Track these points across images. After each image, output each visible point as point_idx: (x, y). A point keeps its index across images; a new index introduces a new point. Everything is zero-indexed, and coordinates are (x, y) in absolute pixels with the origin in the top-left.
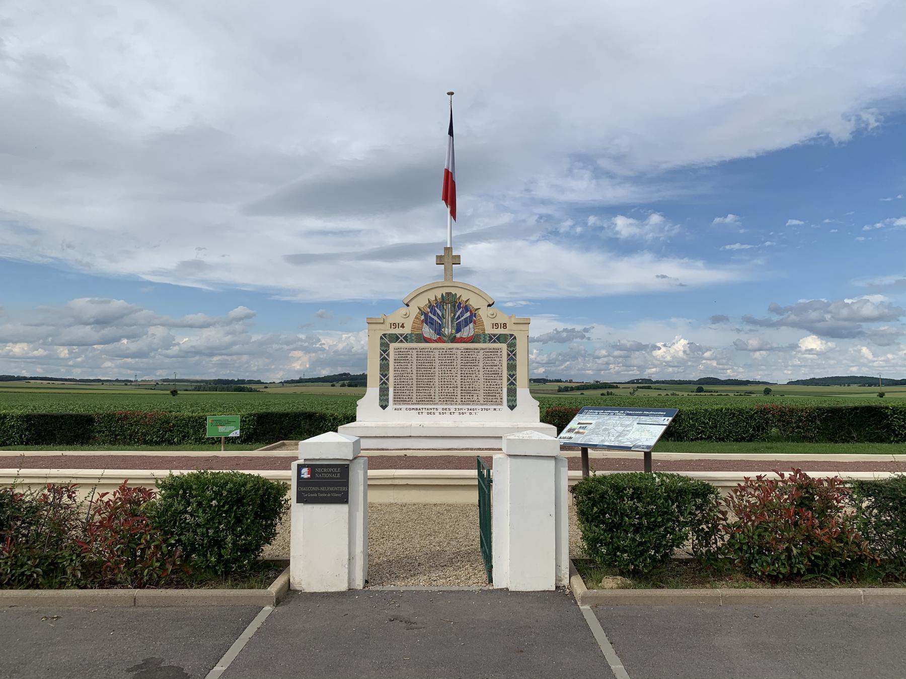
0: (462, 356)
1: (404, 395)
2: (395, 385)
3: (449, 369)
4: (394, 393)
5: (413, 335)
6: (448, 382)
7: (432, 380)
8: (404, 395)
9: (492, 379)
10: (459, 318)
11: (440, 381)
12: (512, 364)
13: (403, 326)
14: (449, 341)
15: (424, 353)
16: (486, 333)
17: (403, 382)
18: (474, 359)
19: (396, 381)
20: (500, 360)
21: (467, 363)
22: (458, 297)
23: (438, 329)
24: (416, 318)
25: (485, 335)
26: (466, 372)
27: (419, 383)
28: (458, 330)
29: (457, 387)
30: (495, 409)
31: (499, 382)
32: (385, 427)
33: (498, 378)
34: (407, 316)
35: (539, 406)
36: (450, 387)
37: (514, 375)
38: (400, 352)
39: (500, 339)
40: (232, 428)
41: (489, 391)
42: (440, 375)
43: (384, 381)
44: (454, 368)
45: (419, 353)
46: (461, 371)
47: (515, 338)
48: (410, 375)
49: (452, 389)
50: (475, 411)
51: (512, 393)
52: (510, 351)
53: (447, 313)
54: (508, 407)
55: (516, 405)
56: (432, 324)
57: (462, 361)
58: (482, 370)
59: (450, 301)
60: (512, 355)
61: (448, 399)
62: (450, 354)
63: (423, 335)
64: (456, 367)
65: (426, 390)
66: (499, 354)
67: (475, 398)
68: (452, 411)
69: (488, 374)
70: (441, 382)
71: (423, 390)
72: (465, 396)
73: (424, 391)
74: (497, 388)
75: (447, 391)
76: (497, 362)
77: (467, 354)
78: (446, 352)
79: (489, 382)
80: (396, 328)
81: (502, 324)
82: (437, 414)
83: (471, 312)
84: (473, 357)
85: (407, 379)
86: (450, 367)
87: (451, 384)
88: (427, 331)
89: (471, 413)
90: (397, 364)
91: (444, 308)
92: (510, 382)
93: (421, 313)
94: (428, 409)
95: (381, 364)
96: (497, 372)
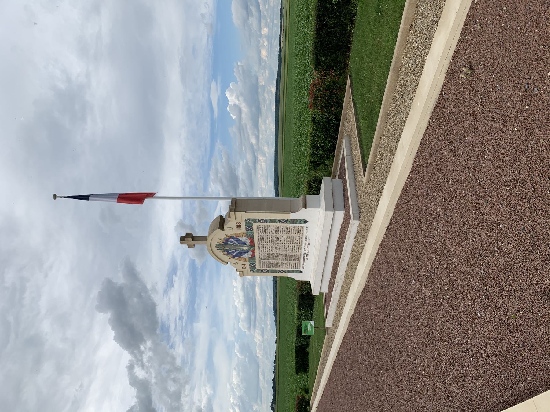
13: (245, 264)
16: (245, 232)
24: (237, 259)
28: (245, 244)
30: (307, 230)
40: (309, 325)
47: (247, 219)
51: (293, 221)
56: (241, 254)
59: (223, 246)
62: (263, 247)
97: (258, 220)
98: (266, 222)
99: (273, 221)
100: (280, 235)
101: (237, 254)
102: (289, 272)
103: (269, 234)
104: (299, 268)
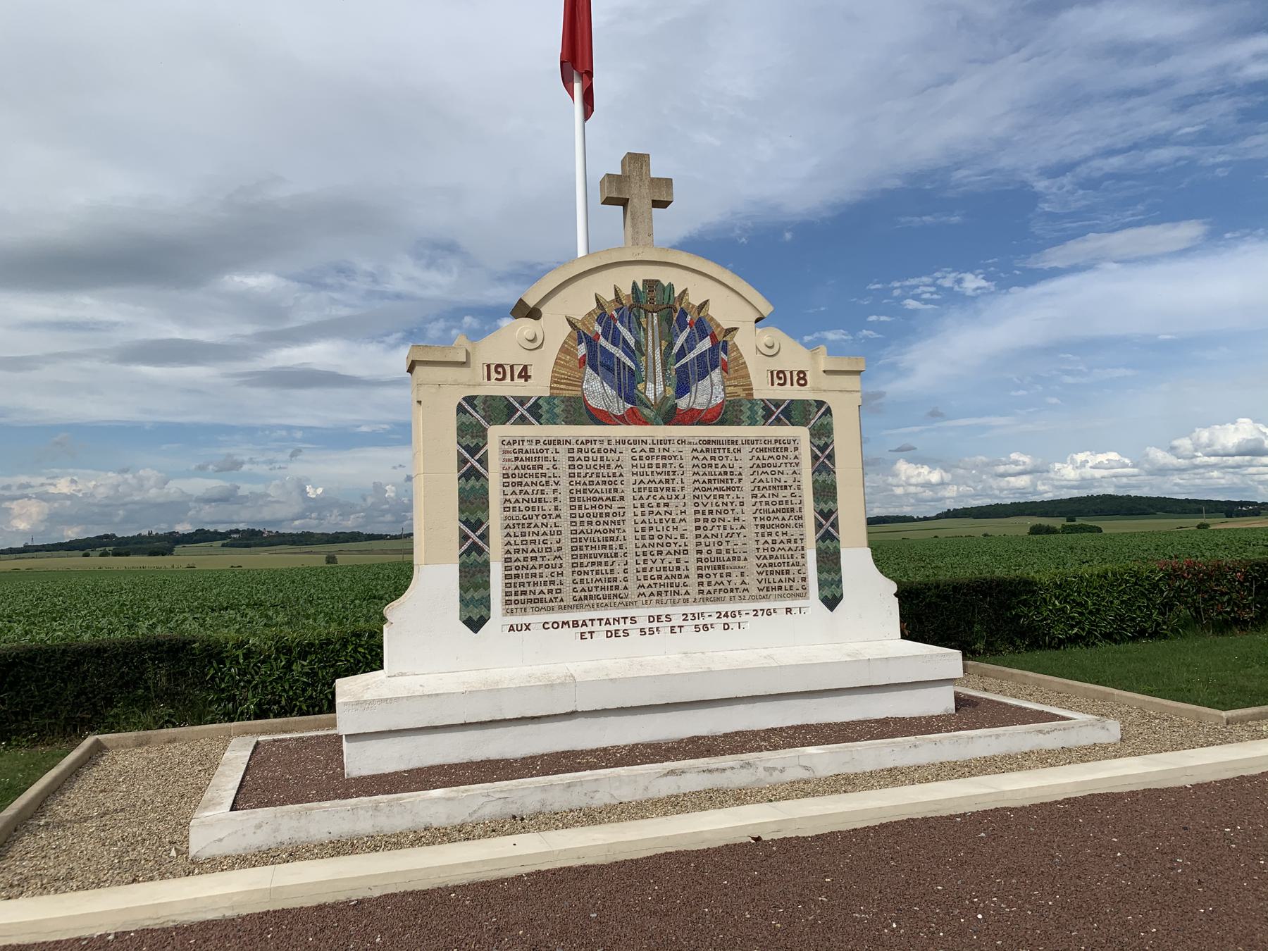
0: (696, 462)
1: (536, 584)
2: (508, 552)
3: (662, 501)
4: (506, 577)
5: (556, 401)
6: (660, 537)
7: (615, 535)
8: (536, 584)
9: (778, 526)
10: (682, 353)
11: (639, 535)
12: (824, 481)
13: (525, 375)
14: (659, 420)
15: (590, 455)
16: (755, 397)
17: (533, 542)
18: (728, 470)
19: (512, 540)
20: (794, 472)
21: (710, 481)
22: (676, 294)
23: (627, 385)
24: (564, 350)
25: (753, 402)
26: (709, 507)
27: (578, 544)
28: (683, 389)
29: (686, 552)
30: (789, 610)
31: (795, 532)
32: (493, 692)
33: (792, 522)
34: (535, 344)
35: (896, 595)
36: (669, 553)
37: (833, 513)
38: (521, 451)
39: (791, 413)
41: (772, 561)
42: (639, 518)
43: (474, 543)
44: (677, 497)
45: (576, 455)
46: (696, 505)
47: (828, 411)
48: (551, 522)
49: (672, 558)
50: (738, 619)
51: (830, 561)
52: (818, 447)
53: (650, 338)
54: (822, 601)
55: (842, 596)
56: (610, 369)
57: (696, 477)
58: (749, 500)
60: (824, 461)
61: (662, 589)
62: (664, 458)
63: (587, 404)
64: (681, 494)
65: (600, 564)
66: (791, 454)
67: (736, 580)
68: (677, 621)
69: (767, 511)
70: (643, 537)
71: (593, 564)
72: (708, 576)
73: (595, 568)
74: (790, 549)
75: (659, 564)
76: (787, 479)
77: (708, 456)
78: (652, 450)
79: (769, 534)
80: (504, 378)
81: (795, 374)
82: (635, 633)
83: (713, 337)
84: (724, 466)
85: (544, 533)
86: (665, 494)
87: (669, 545)
88: (597, 391)
89: (726, 627)
90: (509, 490)
91: (640, 324)
92: (822, 531)
93: (576, 336)
94: (608, 622)
95: (461, 491)
96: (790, 506)
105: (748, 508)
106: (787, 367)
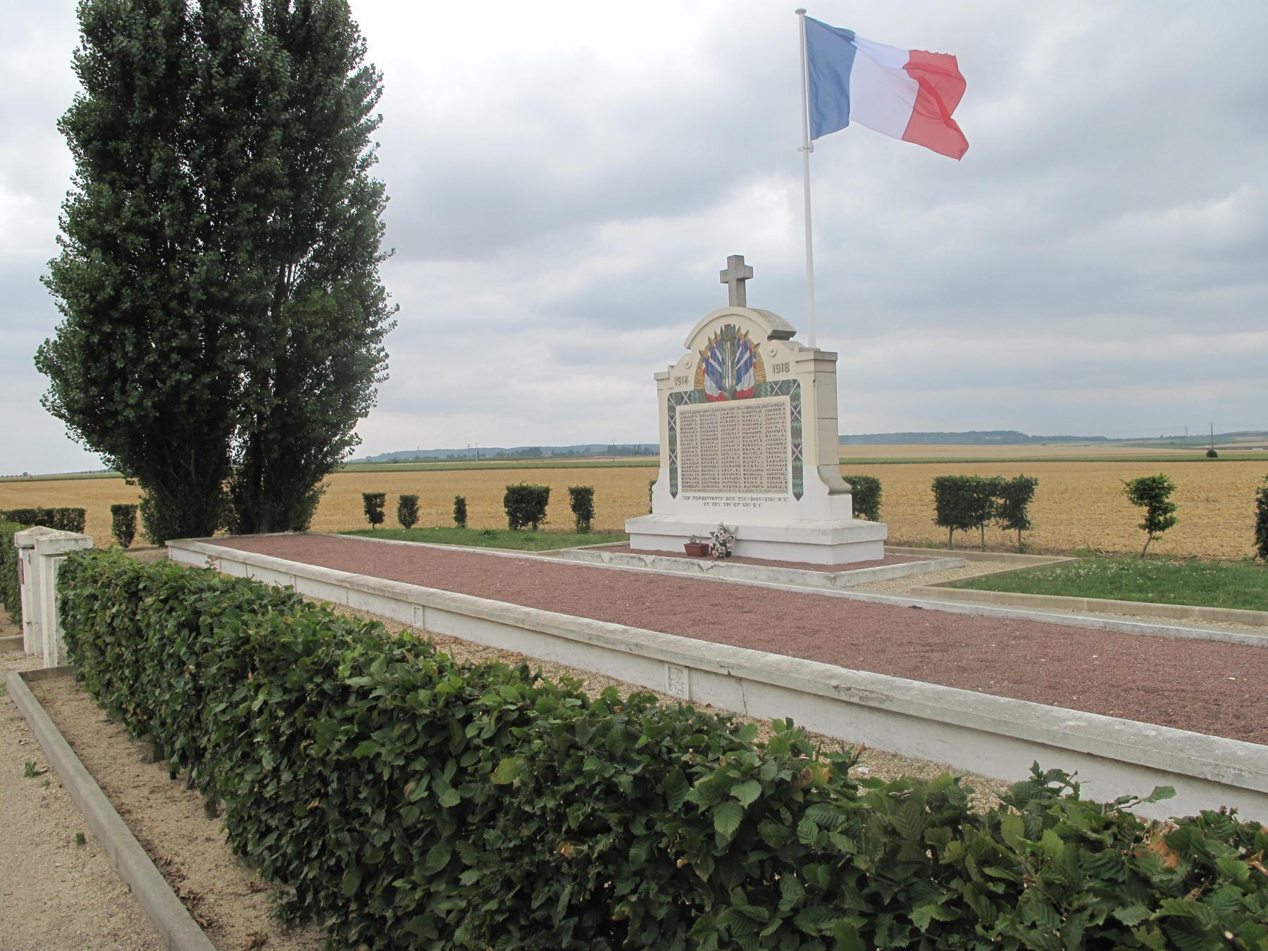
13: (686, 382)
23: (718, 380)
24: (699, 367)
28: (739, 380)
30: (780, 499)
47: (799, 385)
51: (798, 472)
58: (764, 438)
59: (730, 338)
67: (758, 481)
68: (736, 501)
88: (710, 386)
97: (797, 406)
98: (793, 421)
99: (797, 433)
100: (763, 448)
101: (713, 366)
102: (673, 472)
103: (764, 427)
104: (683, 491)
105: (764, 443)
106: (777, 363)
